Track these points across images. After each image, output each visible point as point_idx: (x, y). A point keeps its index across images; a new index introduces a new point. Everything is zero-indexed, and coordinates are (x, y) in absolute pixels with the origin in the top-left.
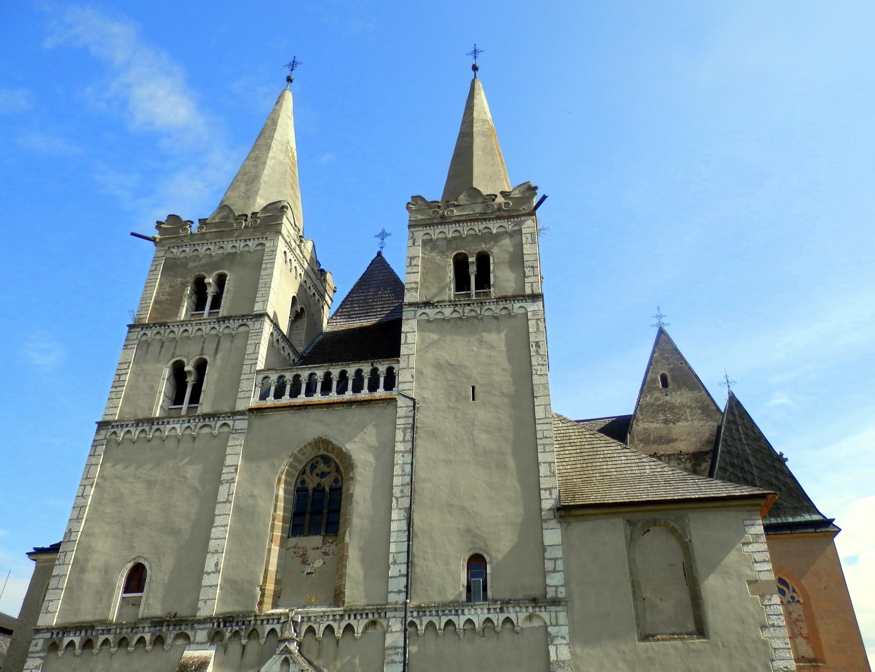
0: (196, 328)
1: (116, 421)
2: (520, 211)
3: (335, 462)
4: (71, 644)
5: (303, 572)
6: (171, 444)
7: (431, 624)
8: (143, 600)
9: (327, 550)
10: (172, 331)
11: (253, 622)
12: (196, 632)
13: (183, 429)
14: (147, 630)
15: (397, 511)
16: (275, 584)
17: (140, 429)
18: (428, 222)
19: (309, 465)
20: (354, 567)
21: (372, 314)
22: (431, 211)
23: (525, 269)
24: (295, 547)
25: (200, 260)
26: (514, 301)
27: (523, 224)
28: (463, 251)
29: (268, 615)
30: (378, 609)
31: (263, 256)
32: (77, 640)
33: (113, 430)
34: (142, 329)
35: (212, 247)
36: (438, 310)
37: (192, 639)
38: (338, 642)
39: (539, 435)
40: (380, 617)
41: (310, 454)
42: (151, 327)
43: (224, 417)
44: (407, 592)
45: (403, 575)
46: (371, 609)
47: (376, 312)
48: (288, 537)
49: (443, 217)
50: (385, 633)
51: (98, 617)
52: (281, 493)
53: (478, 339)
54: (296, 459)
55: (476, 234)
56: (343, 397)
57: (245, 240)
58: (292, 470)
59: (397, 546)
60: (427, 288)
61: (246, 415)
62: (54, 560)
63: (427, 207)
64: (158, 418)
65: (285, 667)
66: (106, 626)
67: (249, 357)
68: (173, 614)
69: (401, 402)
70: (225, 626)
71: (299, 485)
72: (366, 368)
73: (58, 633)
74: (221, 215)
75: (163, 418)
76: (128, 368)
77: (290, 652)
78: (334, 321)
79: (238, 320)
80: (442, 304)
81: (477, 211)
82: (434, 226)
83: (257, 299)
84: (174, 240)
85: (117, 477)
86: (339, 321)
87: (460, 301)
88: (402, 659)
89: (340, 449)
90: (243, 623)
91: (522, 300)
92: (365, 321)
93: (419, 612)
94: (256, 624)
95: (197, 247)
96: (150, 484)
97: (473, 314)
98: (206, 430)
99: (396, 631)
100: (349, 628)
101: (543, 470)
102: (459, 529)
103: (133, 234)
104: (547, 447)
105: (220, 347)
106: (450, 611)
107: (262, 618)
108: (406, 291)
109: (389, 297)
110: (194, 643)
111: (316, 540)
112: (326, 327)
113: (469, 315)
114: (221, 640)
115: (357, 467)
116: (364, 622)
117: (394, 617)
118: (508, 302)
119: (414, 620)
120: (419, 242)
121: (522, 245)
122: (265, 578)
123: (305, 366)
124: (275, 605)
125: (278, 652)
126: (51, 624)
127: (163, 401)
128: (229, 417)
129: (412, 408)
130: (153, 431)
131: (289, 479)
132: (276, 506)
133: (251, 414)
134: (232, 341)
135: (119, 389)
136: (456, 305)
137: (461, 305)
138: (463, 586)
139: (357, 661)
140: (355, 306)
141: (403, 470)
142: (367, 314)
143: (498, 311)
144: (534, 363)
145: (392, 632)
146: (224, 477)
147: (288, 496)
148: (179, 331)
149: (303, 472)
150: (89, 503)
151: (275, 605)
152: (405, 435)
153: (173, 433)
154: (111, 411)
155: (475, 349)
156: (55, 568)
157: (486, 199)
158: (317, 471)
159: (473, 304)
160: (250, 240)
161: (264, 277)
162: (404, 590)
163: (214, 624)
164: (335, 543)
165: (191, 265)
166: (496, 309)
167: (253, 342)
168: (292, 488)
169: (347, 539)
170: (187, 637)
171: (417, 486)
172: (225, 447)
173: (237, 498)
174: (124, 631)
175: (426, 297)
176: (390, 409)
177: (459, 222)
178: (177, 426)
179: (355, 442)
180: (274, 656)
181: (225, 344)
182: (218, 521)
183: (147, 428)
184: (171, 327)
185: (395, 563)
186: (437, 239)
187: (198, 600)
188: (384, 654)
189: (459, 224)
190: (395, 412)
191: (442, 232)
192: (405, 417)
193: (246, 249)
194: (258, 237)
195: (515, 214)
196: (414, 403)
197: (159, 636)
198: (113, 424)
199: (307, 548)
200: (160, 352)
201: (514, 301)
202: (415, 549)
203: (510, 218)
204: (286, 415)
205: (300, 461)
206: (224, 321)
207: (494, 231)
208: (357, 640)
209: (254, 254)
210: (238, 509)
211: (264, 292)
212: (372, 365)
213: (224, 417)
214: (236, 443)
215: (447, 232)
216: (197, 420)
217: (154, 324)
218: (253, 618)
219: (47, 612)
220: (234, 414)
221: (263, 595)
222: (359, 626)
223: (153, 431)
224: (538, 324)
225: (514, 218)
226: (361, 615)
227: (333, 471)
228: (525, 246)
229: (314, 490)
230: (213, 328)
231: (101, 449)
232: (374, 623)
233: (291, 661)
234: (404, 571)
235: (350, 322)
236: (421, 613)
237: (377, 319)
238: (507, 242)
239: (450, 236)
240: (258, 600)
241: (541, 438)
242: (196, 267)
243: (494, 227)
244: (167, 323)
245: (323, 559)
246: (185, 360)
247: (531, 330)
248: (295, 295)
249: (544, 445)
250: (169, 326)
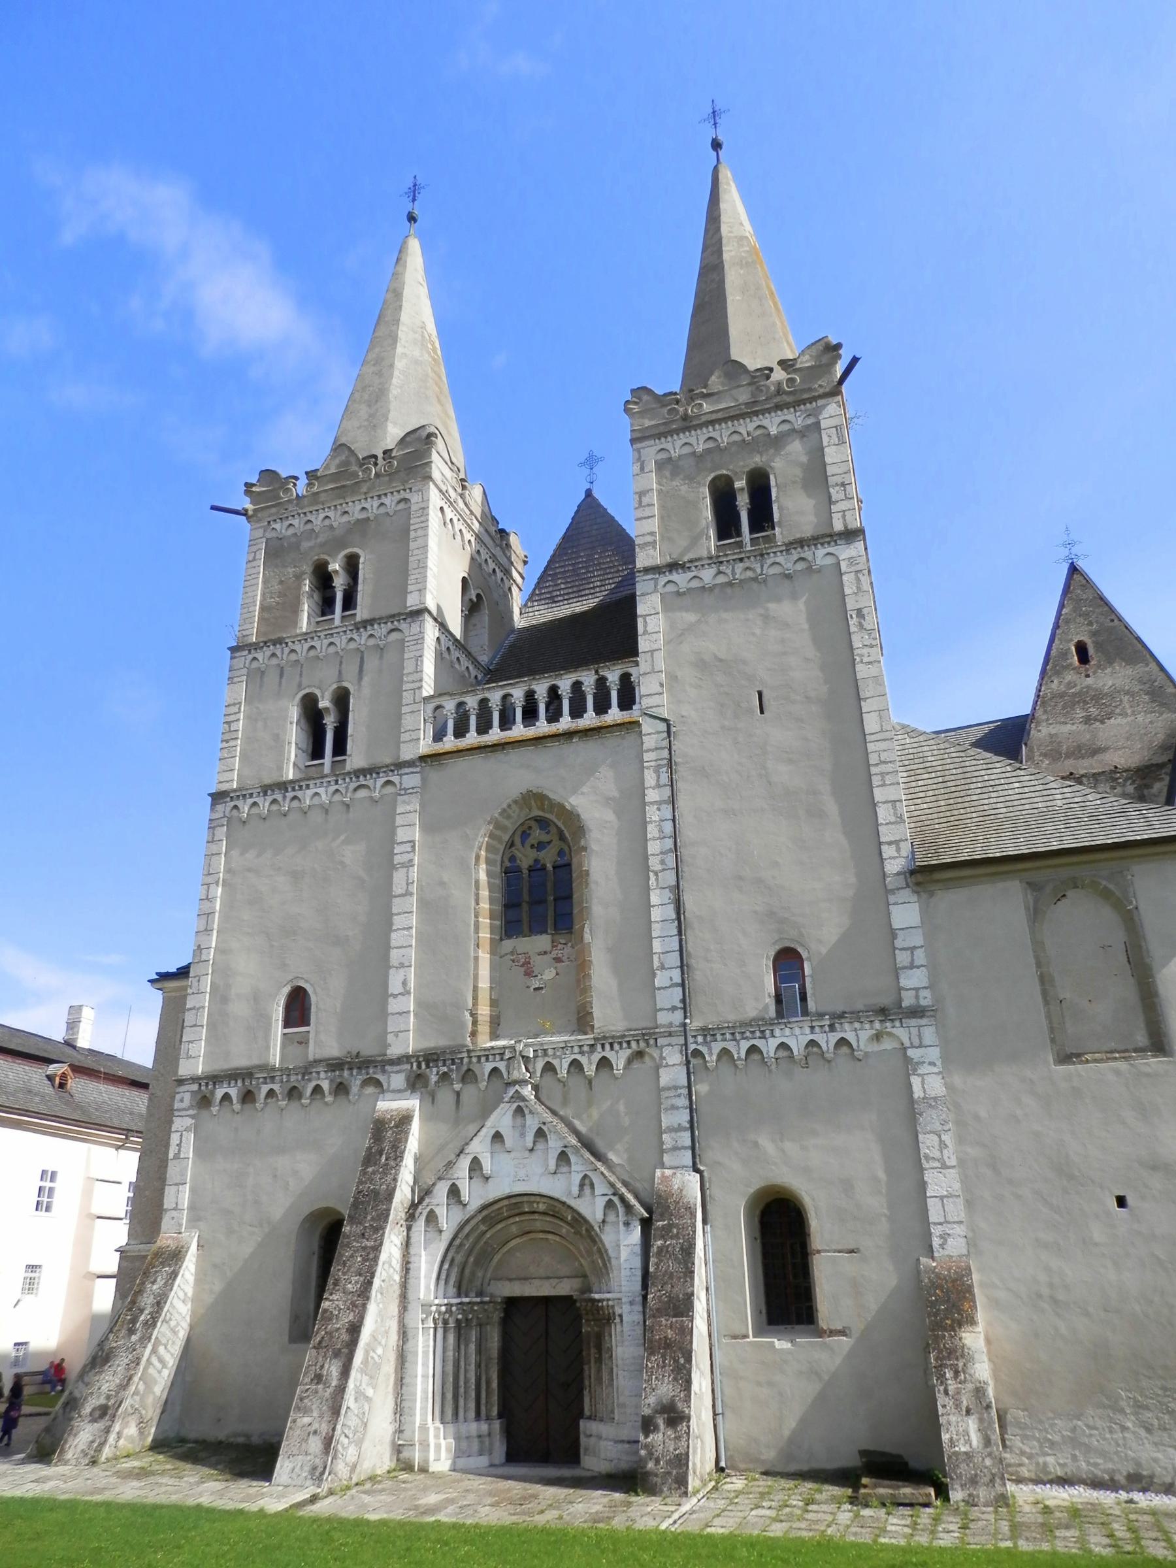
0: (326, 642)
1: (235, 791)
2: (815, 390)
3: (557, 826)
4: (226, 1097)
5: (528, 987)
6: (316, 817)
7: (725, 1052)
8: (312, 1036)
9: (560, 955)
10: (293, 651)
11: (466, 1060)
12: (389, 1077)
13: (329, 795)
14: (322, 1075)
15: (658, 891)
16: (491, 1006)
17: (269, 799)
18: (662, 429)
19: (519, 833)
20: (602, 976)
21: (587, 592)
22: (665, 410)
23: (831, 490)
24: (512, 953)
25: (317, 537)
26: (815, 545)
27: (820, 413)
28: (725, 472)
29: (485, 1050)
30: (644, 1035)
31: (410, 519)
32: (233, 1092)
33: (232, 804)
34: (250, 651)
35: (331, 514)
36: (692, 574)
37: (385, 1086)
38: (590, 1082)
39: (873, 759)
40: (648, 1044)
41: (518, 816)
42: (262, 647)
43: (384, 772)
44: (684, 1009)
45: (676, 985)
46: (633, 1036)
47: (594, 588)
48: (501, 940)
49: (685, 418)
50: (657, 1068)
51: (255, 1061)
52: (483, 876)
53: (761, 615)
54: (498, 826)
55: (744, 440)
56: (558, 727)
57: (379, 496)
58: (495, 843)
59: (663, 943)
60: (670, 540)
61: (417, 766)
62: (185, 988)
63: (658, 405)
64: (292, 782)
65: (519, 1120)
66: (271, 1075)
67: (410, 678)
68: (354, 1053)
69: (647, 726)
70: (428, 1066)
71: (508, 864)
72: (588, 679)
73: (207, 1084)
74: (337, 461)
75: (298, 781)
76: (239, 712)
77: (524, 1099)
78: (531, 609)
79: (386, 623)
80: (697, 564)
81: (741, 401)
82: (672, 436)
83: (410, 588)
84: (274, 510)
85: (249, 870)
86: (538, 608)
87: (726, 555)
88: (687, 1103)
89: (561, 806)
90: (453, 1063)
91: (829, 543)
92: (578, 604)
93: (705, 1036)
94: (470, 1062)
95: (309, 517)
96: (296, 876)
97: (749, 574)
98: (362, 793)
99: (674, 1065)
100: (604, 1063)
101: (884, 814)
102: (756, 912)
103: (214, 508)
104: (887, 777)
105: (365, 666)
106: (753, 1032)
107: (478, 1054)
108: (637, 550)
109: (611, 561)
110: (389, 1091)
111: (542, 941)
112: (519, 622)
113: (743, 577)
114: (426, 1085)
115: (590, 831)
116: (625, 1054)
117: (669, 1045)
118: (806, 548)
119: (699, 1047)
121: (822, 449)
122: (475, 998)
123: (494, 685)
124: (494, 1036)
125: (506, 1099)
126: (195, 1073)
127: (296, 756)
128: (392, 771)
129: (665, 735)
130: (288, 800)
131: (491, 856)
132: (477, 895)
133: (423, 765)
134: (381, 657)
135: (232, 743)
136: (721, 562)
137: (728, 561)
138: (770, 996)
139: (621, 1107)
140: (559, 582)
141: (661, 831)
142: (580, 594)
143: (790, 565)
144: (857, 643)
145: (667, 1066)
146: (397, 859)
147: (492, 880)
148: (302, 649)
149: (511, 844)
150: (218, 908)
151: (494, 1036)
152: (658, 777)
153: (316, 801)
154: (226, 776)
155: (758, 631)
156: (189, 997)
157: (754, 377)
158: (532, 840)
159: (749, 558)
160: (385, 495)
161: (416, 552)
162: (681, 1005)
163: (412, 1064)
164: (570, 944)
165: (305, 545)
166: (787, 562)
167: (412, 655)
168: (498, 869)
169: (587, 937)
170: (378, 1084)
171: (685, 852)
172: (392, 815)
173: (420, 888)
174: (293, 1078)
175: (670, 555)
176: (631, 738)
177: (712, 423)
178: (321, 790)
179: (583, 794)
180: (502, 1105)
181: (372, 663)
182: (398, 921)
183: (279, 797)
184: (290, 644)
185: (662, 967)
186: (680, 456)
187: (386, 1033)
188: (659, 1096)
189: (713, 426)
190: (639, 742)
191: (686, 443)
192: (657, 749)
193: (382, 510)
194: (398, 489)
195: (806, 396)
196: (669, 726)
197: (341, 1083)
198: (232, 795)
199: (531, 953)
200: (280, 683)
201: (815, 545)
202: (690, 946)
203: (799, 405)
204: (477, 760)
205: (503, 828)
206: (365, 628)
207: (774, 431)
208: (617, 1078)
209: (394, 518)
210: (424, 903)
211: (418, 576)
212: (597, 672)
213: (384, 772)
214: (408, 808)
215: (695, 444)
216: (347, 780)
217: (265, 643)
218: (465, 1055)
219: (189, 1057)
220: (399, 765)
221: (475, 1023)
222: (619, 1059)
223: (288, 800)
224: (858, 580)
225: (805, 404)
226: (620, 1043)
227: (555, 839)
228: (826, 450)
229: (531, 870)
230: (351, 639)
231: (221, 832)
232: (640, 1054)
233: (526, 1111)
234: (677, 979)
235: (555, 609)
236: (709, 1038)
237: (597, 600)
238: (796, 447)
239: (700, 449)
240: (470, 1030)
241: (877, 765)
242: (311, 548)
243: (773, 424)
244: (284, 638)
245: (556, 968)
246: (318, 692)
247: (847, 591)
248: (466, 575)
249: (882, 774)
250: (287, 643)
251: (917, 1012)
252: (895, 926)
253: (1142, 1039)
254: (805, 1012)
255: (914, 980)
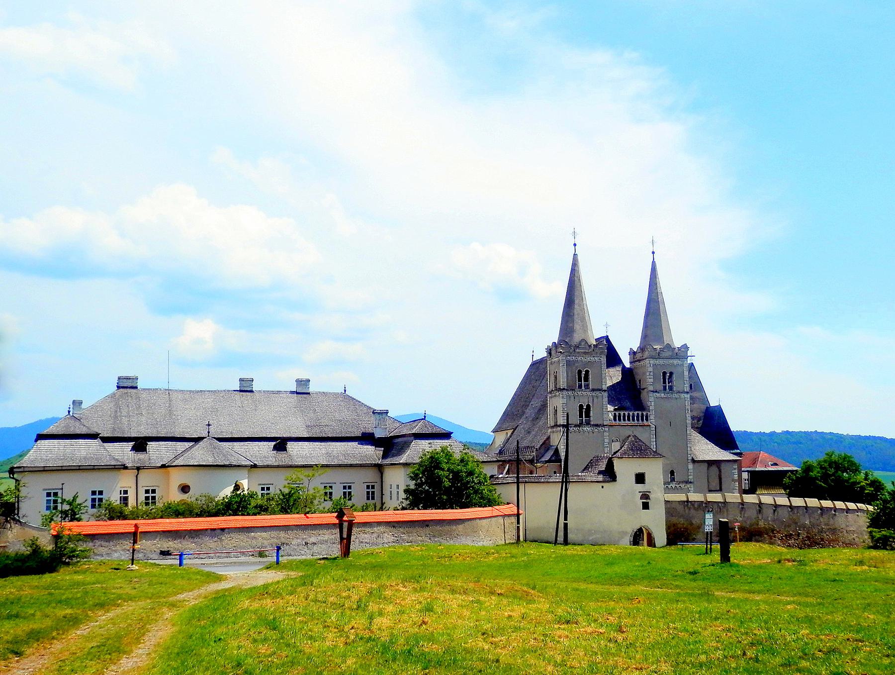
72: (640, 413)
120: (652, 365)
166: (676, 396)
220: (604, 426)
251: (691, 483)
252: (689, 468)
253: (718, 489)
254: (674, 481)
255: (691, 477)
